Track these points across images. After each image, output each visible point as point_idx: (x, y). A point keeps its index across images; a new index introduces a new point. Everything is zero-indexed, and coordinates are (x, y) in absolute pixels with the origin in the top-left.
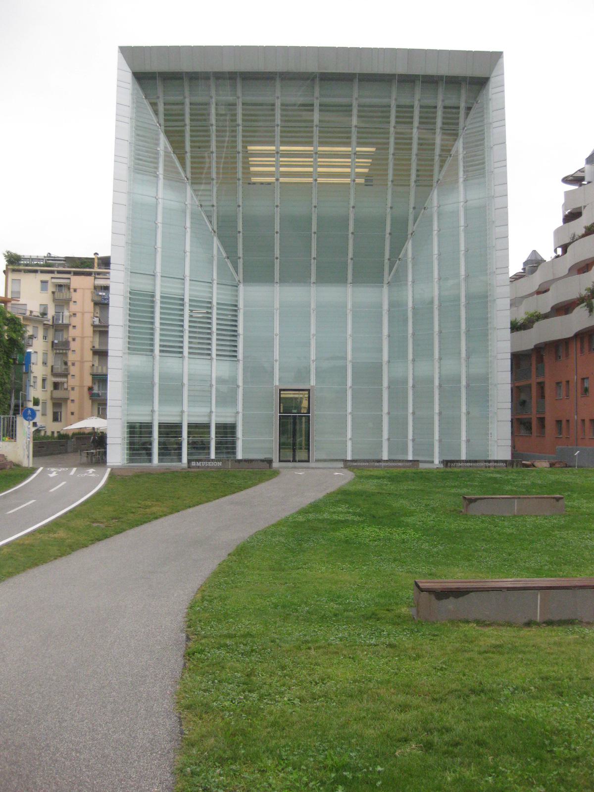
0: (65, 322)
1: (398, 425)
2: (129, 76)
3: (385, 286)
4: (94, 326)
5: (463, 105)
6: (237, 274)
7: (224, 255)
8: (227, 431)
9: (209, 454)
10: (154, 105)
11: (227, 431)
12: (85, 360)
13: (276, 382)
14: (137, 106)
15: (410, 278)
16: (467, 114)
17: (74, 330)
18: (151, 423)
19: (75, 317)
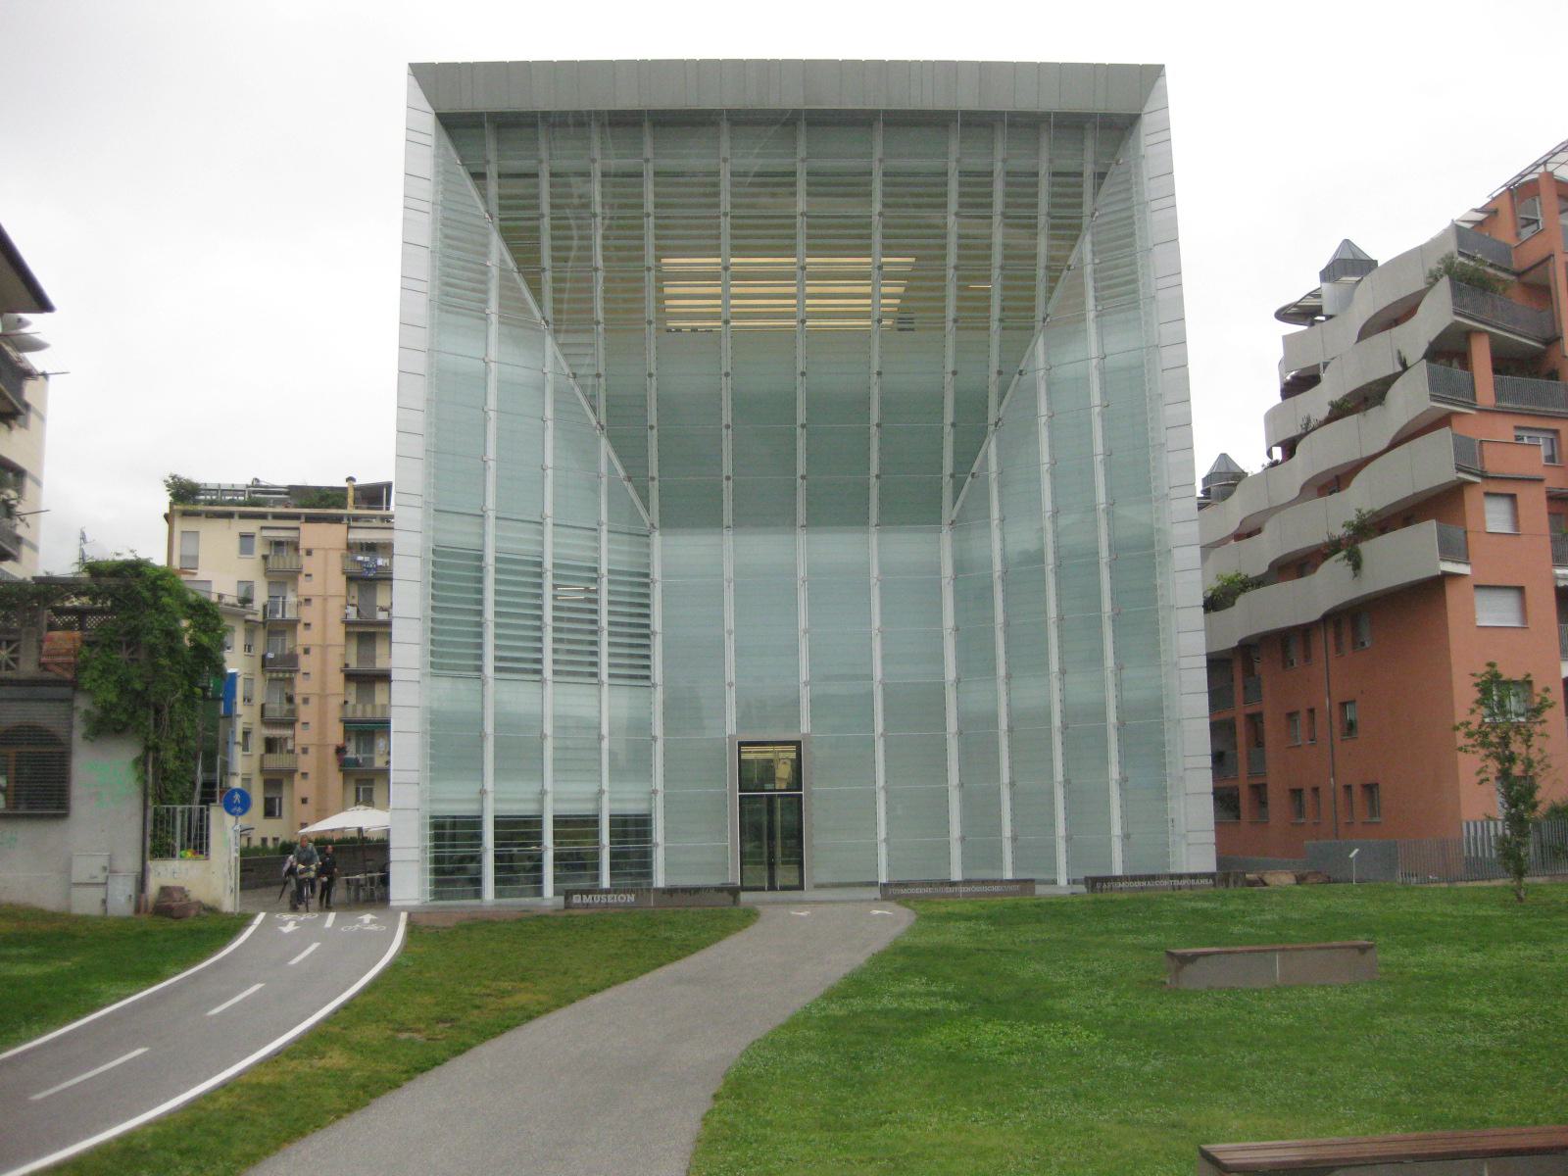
0: (288, 616)
1: (981, 809)
2: (428, 121)
3: (946, 529)
4: (348, 624)
5: (1089, 170)
6: (648, 510)
7: (622, 473)
8: (633, 830)
9: (597, 877)
10: (478, 176)
11: (633, 830)
12: (328, 692)
13: (731, 728)
14: (444, 175)
15: (995, 514)
16: (1098, 187)
17: (307, 632)
18: (479, 817)
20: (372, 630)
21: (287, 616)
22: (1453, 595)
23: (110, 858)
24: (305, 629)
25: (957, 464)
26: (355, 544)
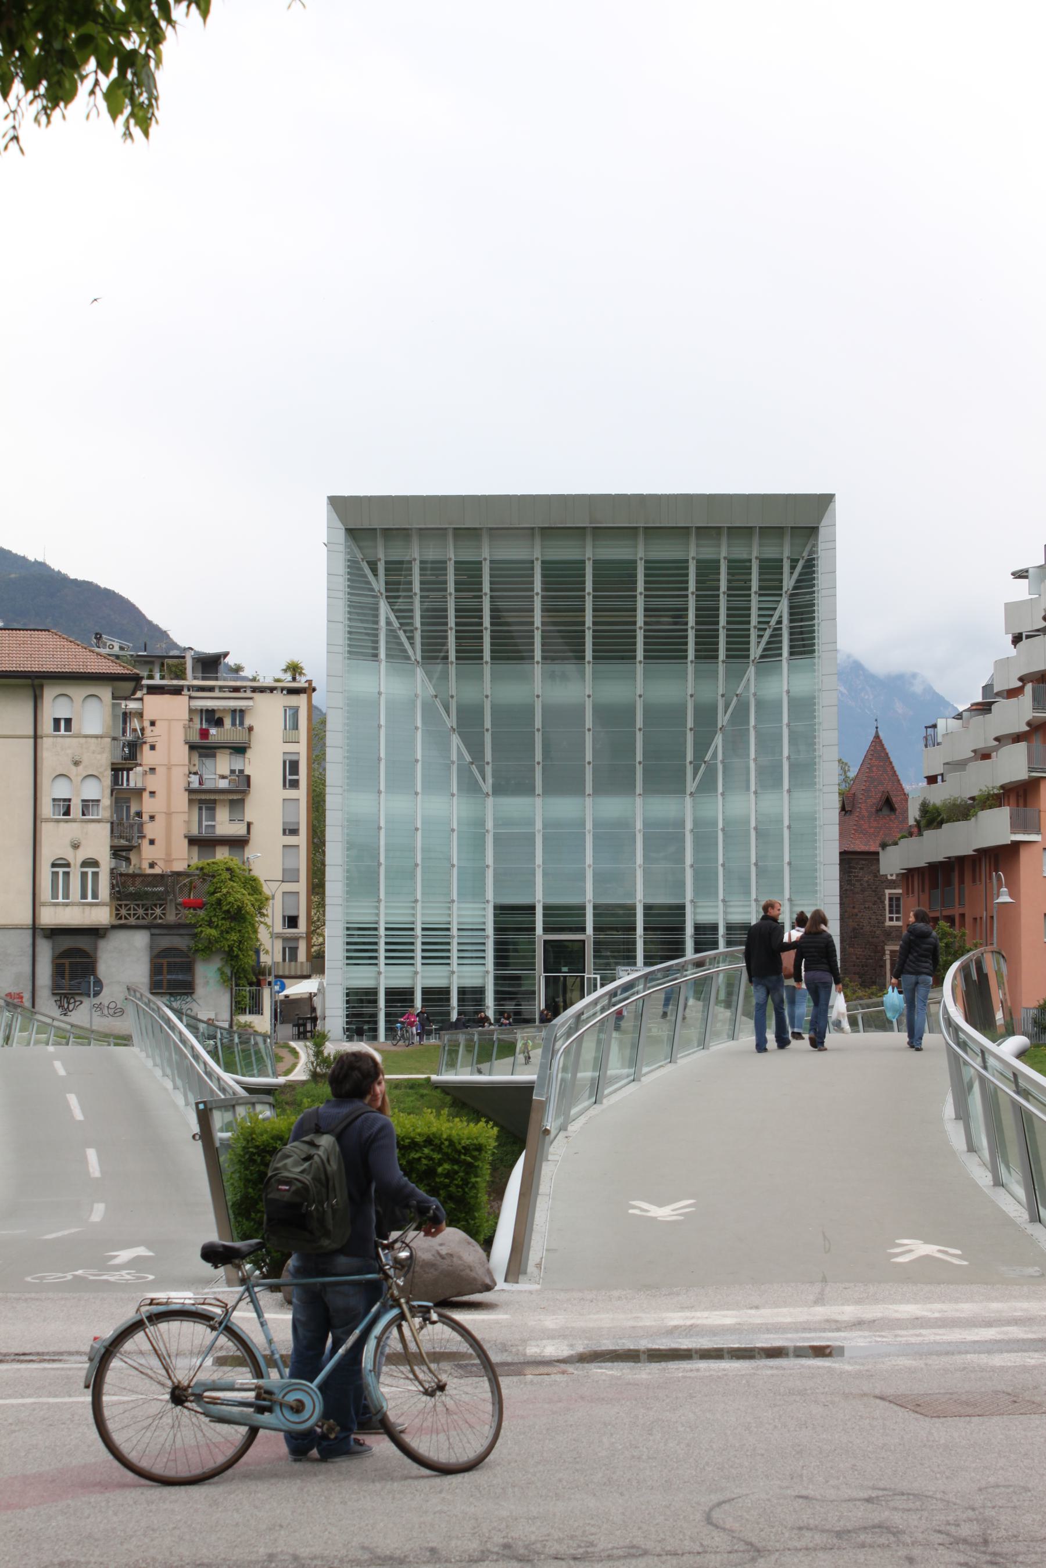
0: (132, 785)
2: (341, 535)
3: (688, 799)
4: (191, 791)
6: (484, 781)
7: (468, 758)
10: (373, 567)
12: (174, 857)
15: (720, 790)
17: (152, 800)
20: (212, 797)
22: (1025, 855)
24: (151, 797)
26: (196, 710)
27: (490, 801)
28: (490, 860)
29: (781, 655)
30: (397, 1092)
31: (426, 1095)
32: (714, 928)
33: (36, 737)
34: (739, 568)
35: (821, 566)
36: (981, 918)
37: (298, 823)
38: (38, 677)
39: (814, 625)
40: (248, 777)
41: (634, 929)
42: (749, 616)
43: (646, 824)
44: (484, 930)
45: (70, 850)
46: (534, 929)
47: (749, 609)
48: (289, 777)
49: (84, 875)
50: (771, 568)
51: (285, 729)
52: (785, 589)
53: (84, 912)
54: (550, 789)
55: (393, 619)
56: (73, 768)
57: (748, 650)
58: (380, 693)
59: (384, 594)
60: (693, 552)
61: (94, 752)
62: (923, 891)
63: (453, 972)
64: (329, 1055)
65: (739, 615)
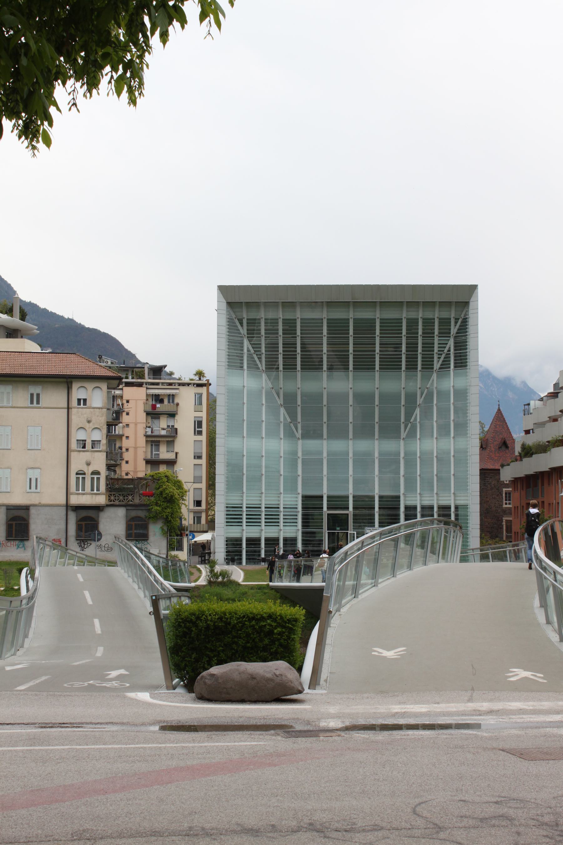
0: (117, 433)
2: (224, 305)
3: (402, 442)
4: (147, 436)
6: (297, 432)
7: (289, 420)
15: (418, 437)
19: (128, 427)
20: (158, 439)
21: (117, 433)
23: (159, 551)
24: (126, 439)
25: (406, 420)
26: (150, 394)
27: (300, 442)
28: (300, 472)
29: (450, 367)
30: (252, 591)
31: (267, 593)
32: (415, 508)
33: (68, 408)
34: (429, 323)
35: (471, 322)
36: (552, 503)
37: (202, 453)
38: (70, 378)
39: (467, 352)
40: (176, 429)
41: (374, 508)
42: (433, 347)
43: (380, 454)
44: (297, 508)
45: (86, 466)
46: (322, 508)
47: (433, 344)
48: (197, 429)
49: (92, 479)
50: (445, 323)
51: (195, 404)
52: (452, 334)
53: (92, 498)
54: (330, 437)
55: (251, 348)
56: (88, 424)
57: (433, 365)
58: (244, 386)
59: (246, 335)
60: (405, 315)
61: (98, 416)
62: (523, 489)
63: (281, 530)
64: (217, 572)
65: (429, 347)
